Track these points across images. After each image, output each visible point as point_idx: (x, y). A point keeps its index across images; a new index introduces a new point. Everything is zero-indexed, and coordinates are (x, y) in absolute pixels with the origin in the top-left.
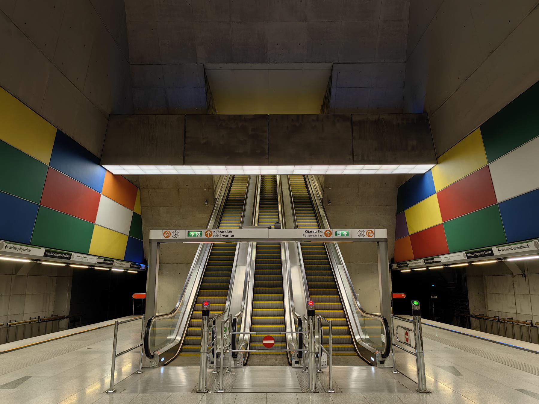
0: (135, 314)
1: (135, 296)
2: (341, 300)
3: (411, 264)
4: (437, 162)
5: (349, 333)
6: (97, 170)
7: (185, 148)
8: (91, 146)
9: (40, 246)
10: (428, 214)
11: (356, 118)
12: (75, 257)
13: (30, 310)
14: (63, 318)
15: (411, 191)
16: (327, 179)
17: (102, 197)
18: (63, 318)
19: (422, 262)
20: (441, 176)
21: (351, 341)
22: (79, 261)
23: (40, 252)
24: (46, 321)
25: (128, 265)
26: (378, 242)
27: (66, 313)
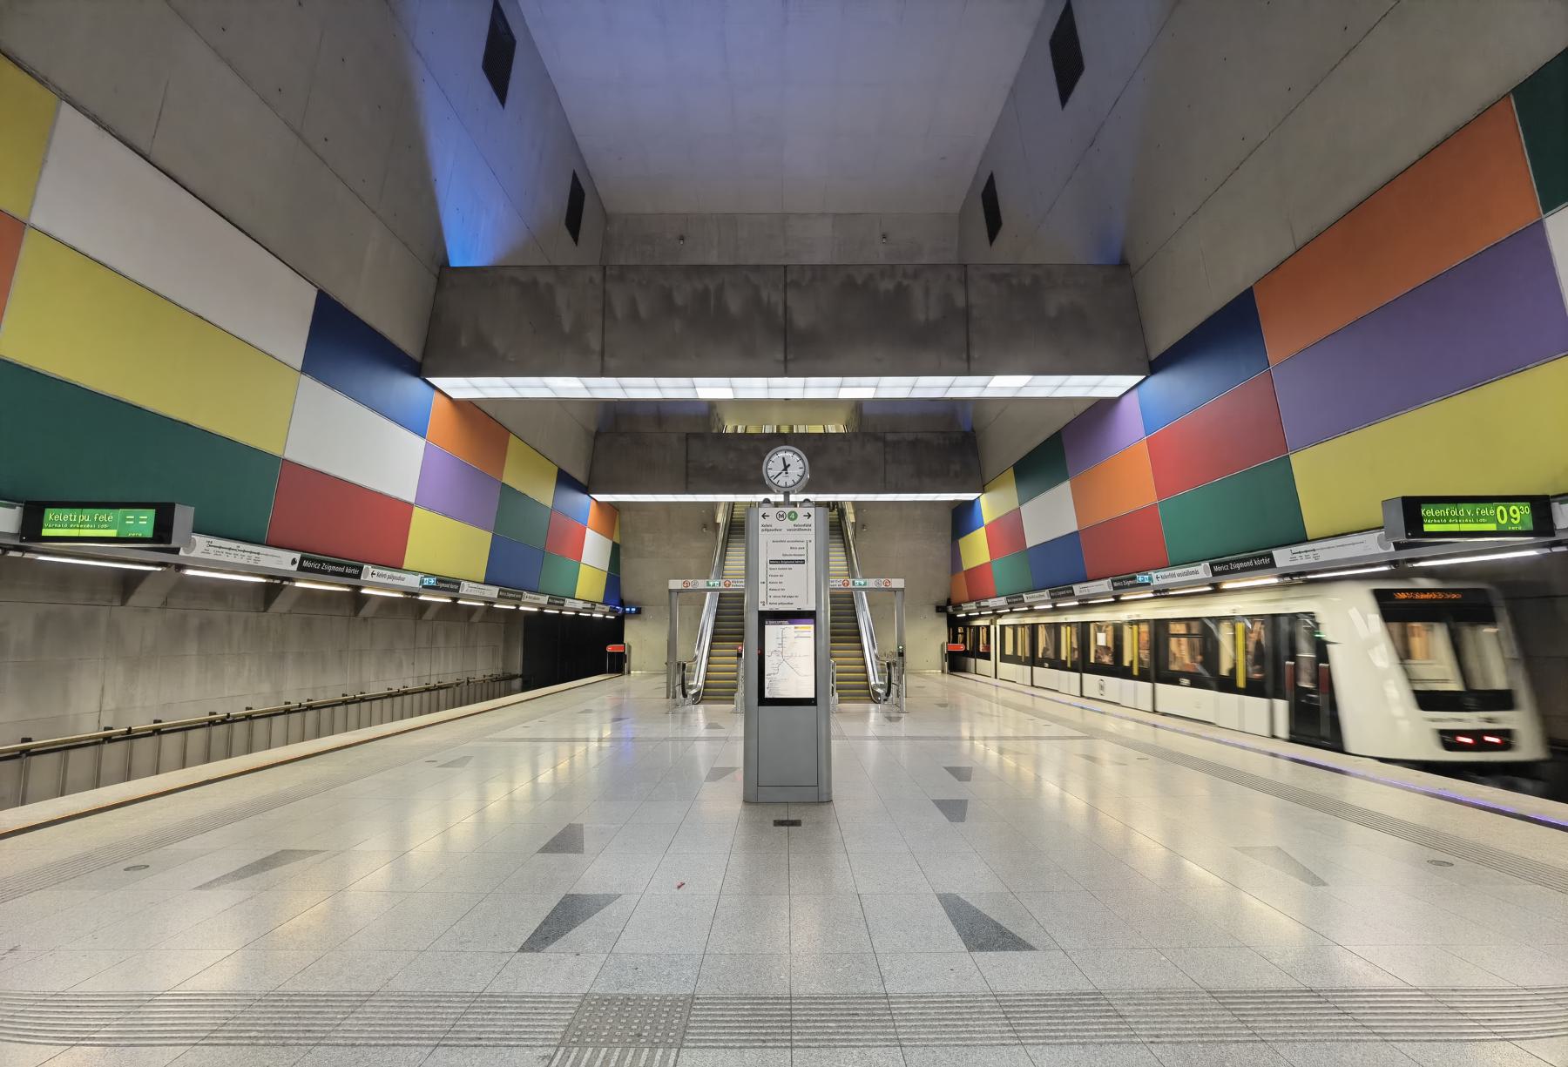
0: (611, 672)
1: (609, 649)
2: (862, 649)
3: (966, 607)
4: (983, 491)
5: (867, 679)
6: (583, 499)
7: (687, 475)
8: (580, 475)
9: (544, 594)
10: (977, 549)
11: (890, 437)
12: (569, 603)
13: (483, 667)
14: (516, 677)
15: (962, 519)
16: (855, 503)
17: (589, 531)
18: (516, 677)
19: (973, 605)
20: (990, 505)
21: (867, 687)
22: (571, 607)
23: (544, 600)
24: (498, 680)
25: (607, 608)
26: (895, 590)
27: (519, 671)
